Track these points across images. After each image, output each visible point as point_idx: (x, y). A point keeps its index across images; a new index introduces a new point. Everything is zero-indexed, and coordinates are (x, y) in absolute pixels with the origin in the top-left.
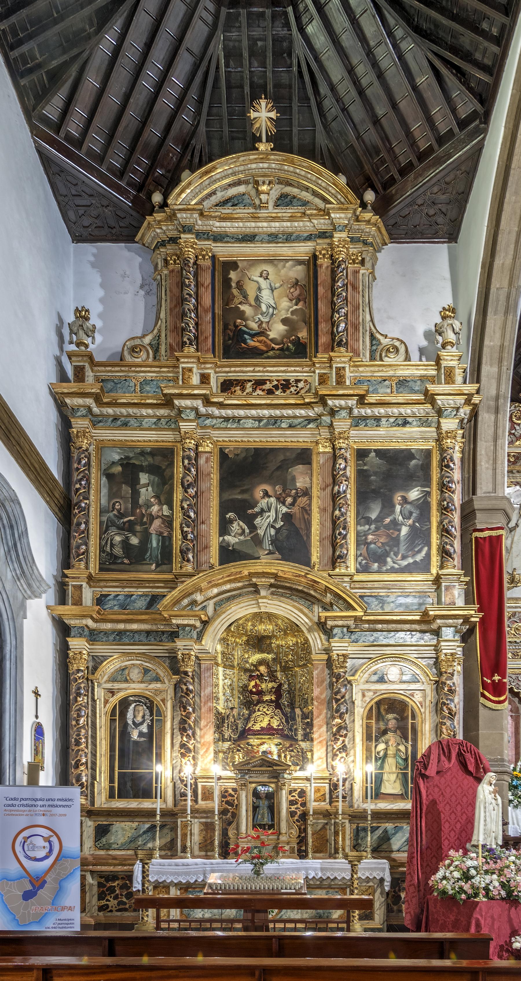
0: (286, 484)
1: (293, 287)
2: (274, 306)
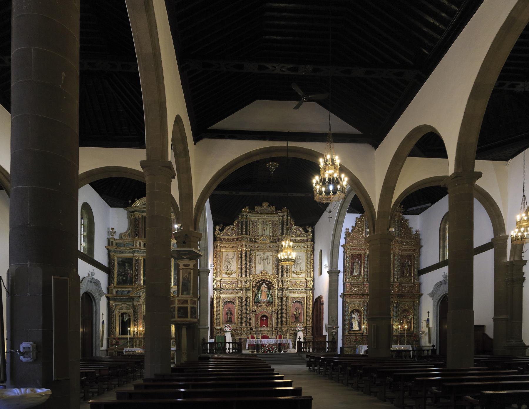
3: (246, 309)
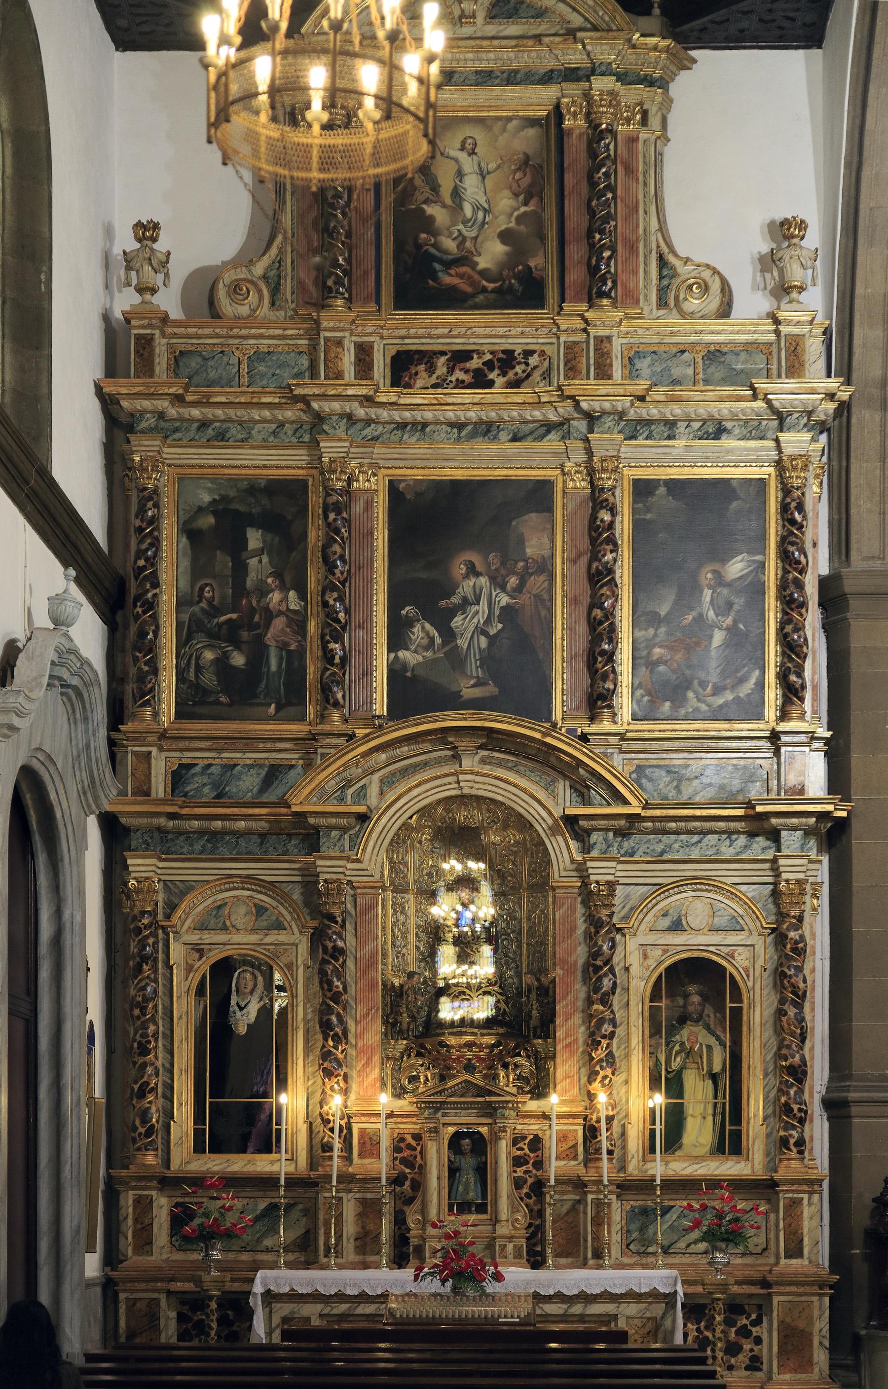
1: (519, 169)
2: (486, 206)
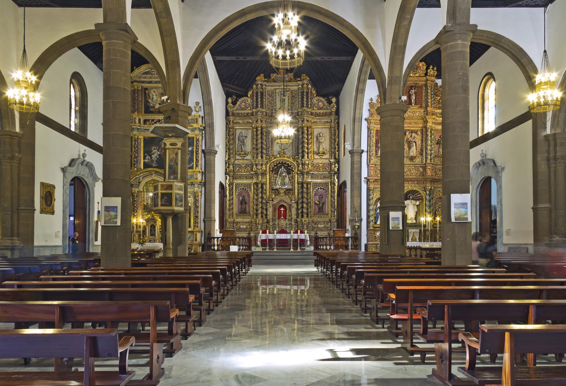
0: (159, 146)
3: (262, 198)
